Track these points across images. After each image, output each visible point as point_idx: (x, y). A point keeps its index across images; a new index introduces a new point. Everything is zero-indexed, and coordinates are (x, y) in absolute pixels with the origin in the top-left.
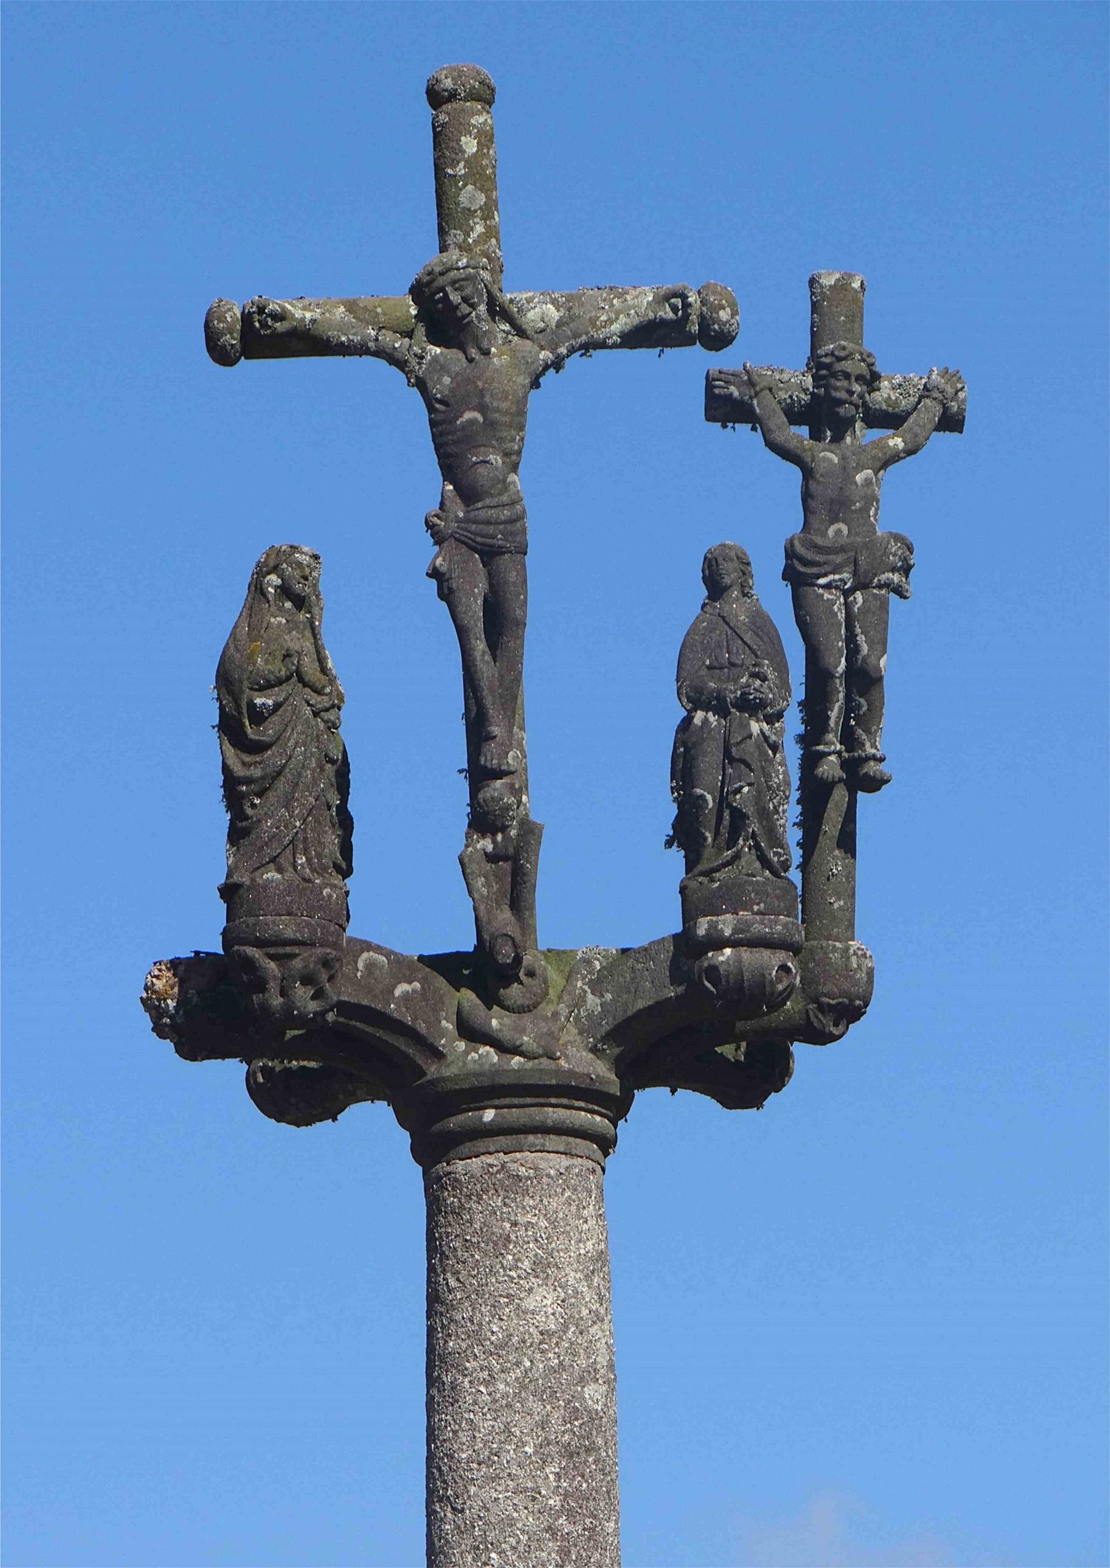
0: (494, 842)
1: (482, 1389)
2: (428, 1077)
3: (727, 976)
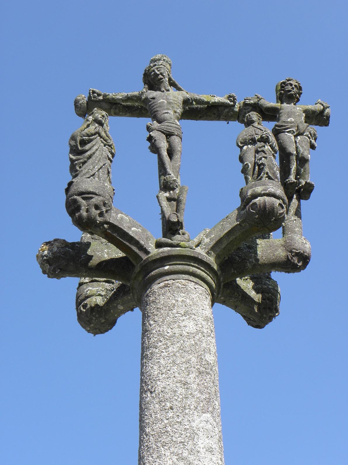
0: (170, 194)
1: (163, 351)
2: (144, 260)
3: (260, 204)
